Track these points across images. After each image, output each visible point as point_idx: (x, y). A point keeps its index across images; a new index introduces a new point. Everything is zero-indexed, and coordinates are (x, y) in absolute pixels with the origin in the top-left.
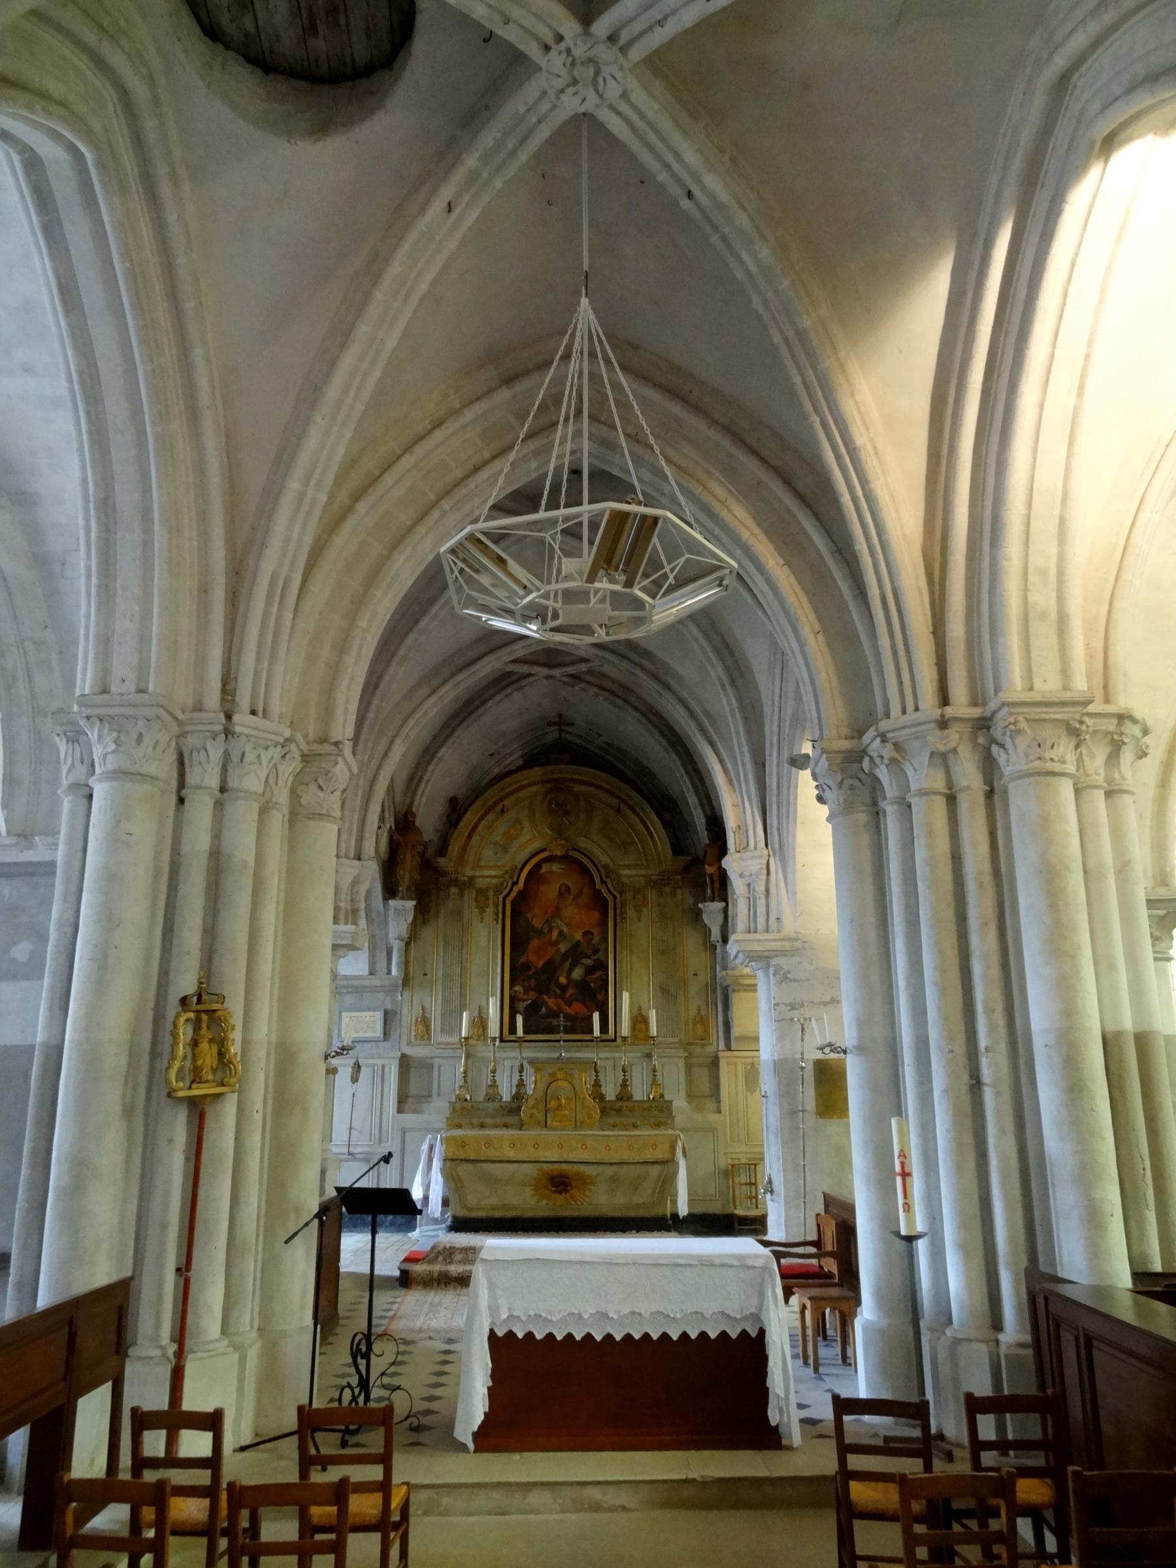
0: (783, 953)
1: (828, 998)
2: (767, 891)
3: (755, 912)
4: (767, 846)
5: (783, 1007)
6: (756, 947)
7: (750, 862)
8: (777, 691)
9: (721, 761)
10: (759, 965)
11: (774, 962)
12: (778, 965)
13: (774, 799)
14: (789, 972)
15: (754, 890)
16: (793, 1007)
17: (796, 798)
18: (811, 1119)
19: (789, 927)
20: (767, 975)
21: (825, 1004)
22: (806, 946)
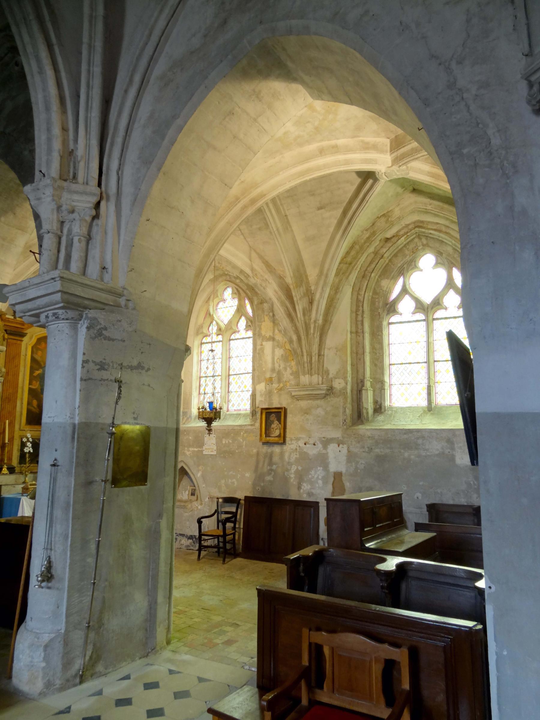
0: (102, 306)
1: (135, 363)
2: (89, 238)
3: (68, 257)
4: (100, 185)
5: (91, 365)
6: (79, 291)
7: (76, 197)
8: (161, 24)
9: (56, 70)
10: (71, 314)
11: (92, 313)
12: (95, 319)
13: (119, 140)
14: (106, 329)
15: (70, 231)
16: (102, 367)
17: (173, 142)
18: (98, 488)
19: (120, 280)
20: (75, 329)
21: (132, 368)
22: (130, 304)
